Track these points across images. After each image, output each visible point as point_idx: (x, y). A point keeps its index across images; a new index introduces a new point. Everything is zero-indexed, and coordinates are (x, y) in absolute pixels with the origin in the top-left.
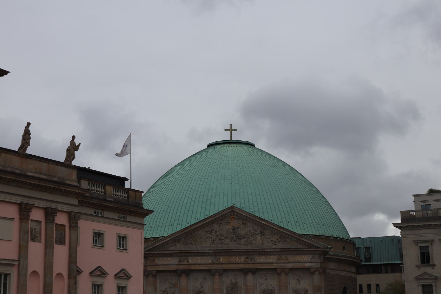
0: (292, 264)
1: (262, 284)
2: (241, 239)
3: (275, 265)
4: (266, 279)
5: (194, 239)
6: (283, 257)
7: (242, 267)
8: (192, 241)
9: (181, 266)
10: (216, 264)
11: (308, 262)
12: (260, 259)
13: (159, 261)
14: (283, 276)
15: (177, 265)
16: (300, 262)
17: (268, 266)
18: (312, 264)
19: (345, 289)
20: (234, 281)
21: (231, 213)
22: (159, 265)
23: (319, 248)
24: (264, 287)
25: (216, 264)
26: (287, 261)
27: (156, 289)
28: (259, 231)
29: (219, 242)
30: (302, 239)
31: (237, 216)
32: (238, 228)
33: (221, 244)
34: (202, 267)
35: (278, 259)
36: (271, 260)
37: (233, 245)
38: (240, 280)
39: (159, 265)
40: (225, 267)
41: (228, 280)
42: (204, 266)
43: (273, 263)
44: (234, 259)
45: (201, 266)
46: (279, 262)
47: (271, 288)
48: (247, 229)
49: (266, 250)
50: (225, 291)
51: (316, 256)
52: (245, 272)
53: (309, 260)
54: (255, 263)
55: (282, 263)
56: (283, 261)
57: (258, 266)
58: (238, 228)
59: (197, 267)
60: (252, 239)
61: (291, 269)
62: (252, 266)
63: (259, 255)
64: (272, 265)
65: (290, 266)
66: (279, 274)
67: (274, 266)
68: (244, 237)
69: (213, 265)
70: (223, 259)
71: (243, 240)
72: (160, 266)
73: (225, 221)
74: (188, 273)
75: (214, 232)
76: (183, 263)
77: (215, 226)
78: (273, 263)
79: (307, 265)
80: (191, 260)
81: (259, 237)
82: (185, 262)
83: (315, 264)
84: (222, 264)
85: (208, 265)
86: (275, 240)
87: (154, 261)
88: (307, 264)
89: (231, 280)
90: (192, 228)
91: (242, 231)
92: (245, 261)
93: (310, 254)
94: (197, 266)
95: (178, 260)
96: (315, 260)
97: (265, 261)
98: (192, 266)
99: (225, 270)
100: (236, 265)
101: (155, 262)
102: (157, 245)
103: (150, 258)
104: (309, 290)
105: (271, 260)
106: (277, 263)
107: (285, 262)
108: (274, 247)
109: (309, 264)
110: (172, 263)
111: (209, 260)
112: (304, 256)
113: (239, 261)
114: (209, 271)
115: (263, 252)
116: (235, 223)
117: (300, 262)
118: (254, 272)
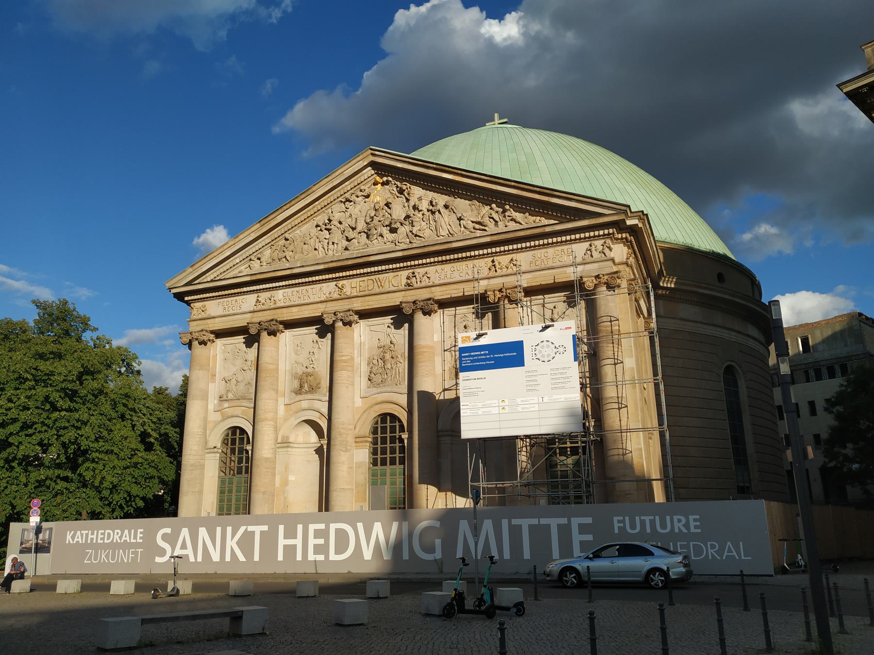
3: (483, 283)
6: (504, 260)
9: (260, 314)
18: (588, 267)
19: (729, 370)
22: (214, 318)
31: (387, 176)
33: (346, 249)
37: (378, 247)
39: (214, 318)
40: (359, 305)
46: (492, 273)
49: (455, 245)
50: (364, 369)
51: (598, 243)
56: (505, 271)
62: (423, 294)
65: (526, 281)
72: (217, 319)
76: (264, 307)
83: (595, 265)
94: (294, 309)
101: (208, 313)
107: (510, 271)
108: (479, 233)
115: (446, 253)
116: (380, 194)
117: (553, 268)
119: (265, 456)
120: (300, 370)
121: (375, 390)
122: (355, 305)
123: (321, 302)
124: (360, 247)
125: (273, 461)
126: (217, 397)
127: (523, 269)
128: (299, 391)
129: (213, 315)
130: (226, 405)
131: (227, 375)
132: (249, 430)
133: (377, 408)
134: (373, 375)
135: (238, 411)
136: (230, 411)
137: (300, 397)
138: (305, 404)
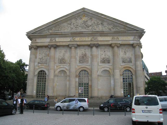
0: (121, 42)
1: (102, 54)
2: (88, 27)
3: (110, 42)
4: (105, 51)
5: (60, 28)
6: (116, 38)
7: (89, 43)
8: (59, 29)
9: (51, 43)
10: (73, 42)
11: (131, 41)
12: (100, 38)
13: (38, 40)
14: (116, 48)
15: (48, 42)
16: (127, 41)
17: (106, 43)
18: (134, 41)
20: (84, 53)
21: (84, 13)
23: (139, 31)
24: (103, 56)
25: (73, 42)
26: (118, 40)
27: (36, 57)
28: (100, 22)
29: (75, 29)
30: (128, 26)
32: (87, 21)
34: (64, 44)
35: (112, 39)
36: (108, 39)
38: (88, 51)
40: (78, 43)
41: (80, 52)
42: (65, 43)
43: (109, 41)
44: (84, 39)
45: (63, 43)
47: (108, 57)
48: (92, 22)
49: (105, 32)
50: (78, 59)
52: (91, 46)
53: (132, 40)
54: (97, 41)
55: (115, 41)
56: (116, 40)
57: (100, 43)
58: (87, 21)
59: (61, 44)
60: (96, 27)
61: (121, 45)
62: (96, 43)
63: (101, 36)
64: (109, 42)
65: (120, 42)
66: (113, 47)
67: (110, 43)
68: (90, 26)
69: (70, 42)
70: (77, 39)
71: (90, 27)
73: (79, 17)
74: (56, 47)
75: (73, 23)
77: (73, 21)
78: (109, 41)
79: (131, 42)
80: (57, 39)
81: (100, 26)
82: (54, 41)
83: (135, 41)
84: (76, 41)
85: (68, 42)
86: (111, 28)
87: (36, 40)
88: (131, 41)
89: (82, 52)
90: (59, 20)
91: (89, 23)
92: (91, 40)
93: (132, 35)
94: (61, 43)
95: (50, 40)
96: (136, 39)
97: (104, 40)
98: (58, 43)
99: (79, 46)
100: (85, 42)
102: (37, 30)
103: (34, 39)
104: (132, 58)
105: (108, 39)
106: (112, 41)
109: (133, 41)
110: (46, 41)
111: (68, 39)
112: (128, 37)
113: (87, 40)
114: (68, 46)
115: (102, 34)
116: (85, 19)
118: (98, 46)
119: (52, 78)
120: (60, 58)
121: (80, 64)
122: (78, 43)
123: (68, 42)
124: (80, 30)
125: (53, 80)
126: (37, 62)
127: (120, 40)
128: (61, 63)
129: (38, 42)
130: (40, 65)
131: (40, 57)
132: (47, 72)
133: (81, 68)
134: (80, 60)
135: (43, 67)
136: (41, 66)
137: (60, 65)
138: (61, 66)
